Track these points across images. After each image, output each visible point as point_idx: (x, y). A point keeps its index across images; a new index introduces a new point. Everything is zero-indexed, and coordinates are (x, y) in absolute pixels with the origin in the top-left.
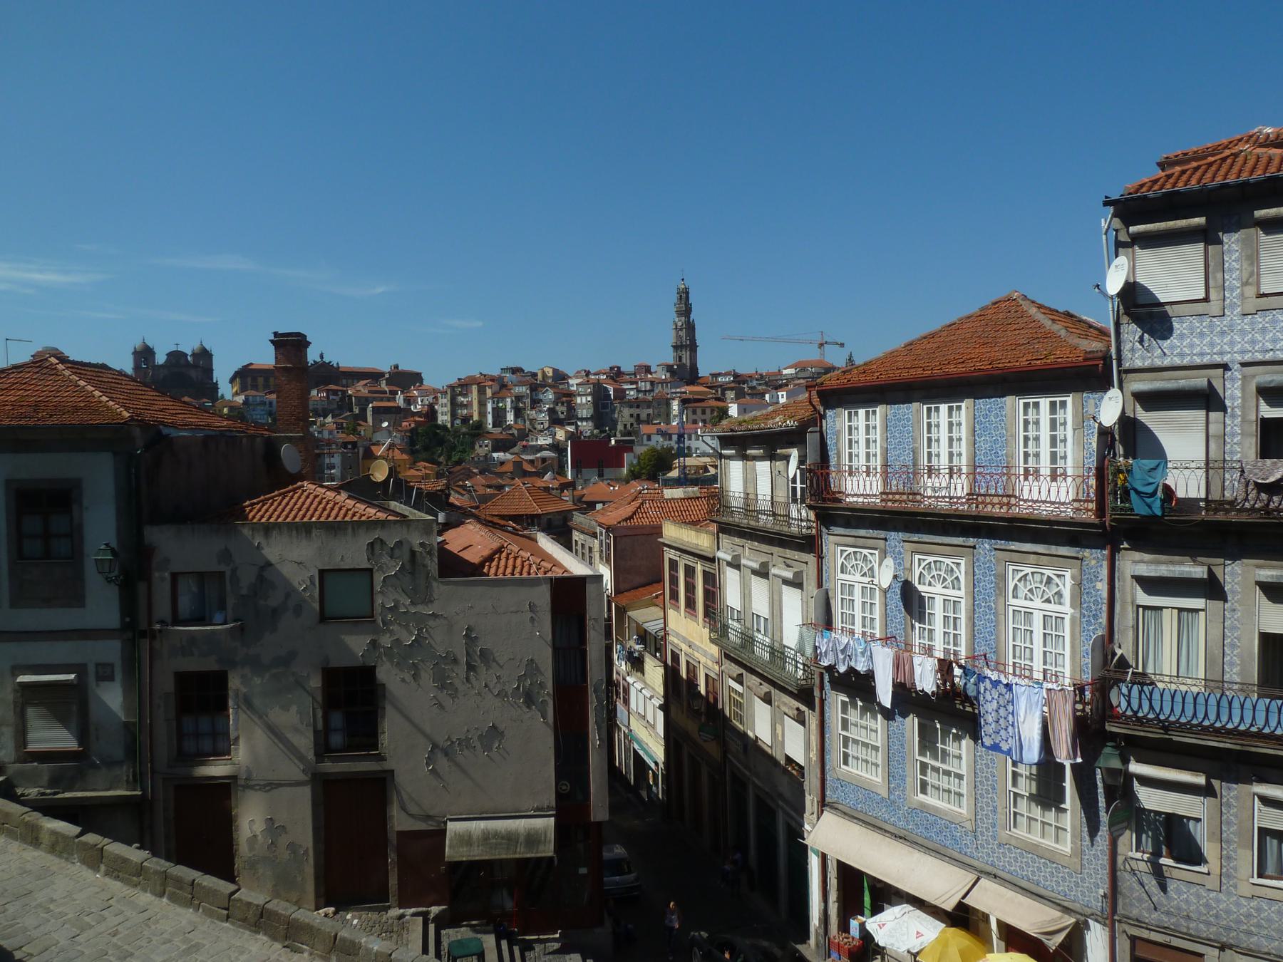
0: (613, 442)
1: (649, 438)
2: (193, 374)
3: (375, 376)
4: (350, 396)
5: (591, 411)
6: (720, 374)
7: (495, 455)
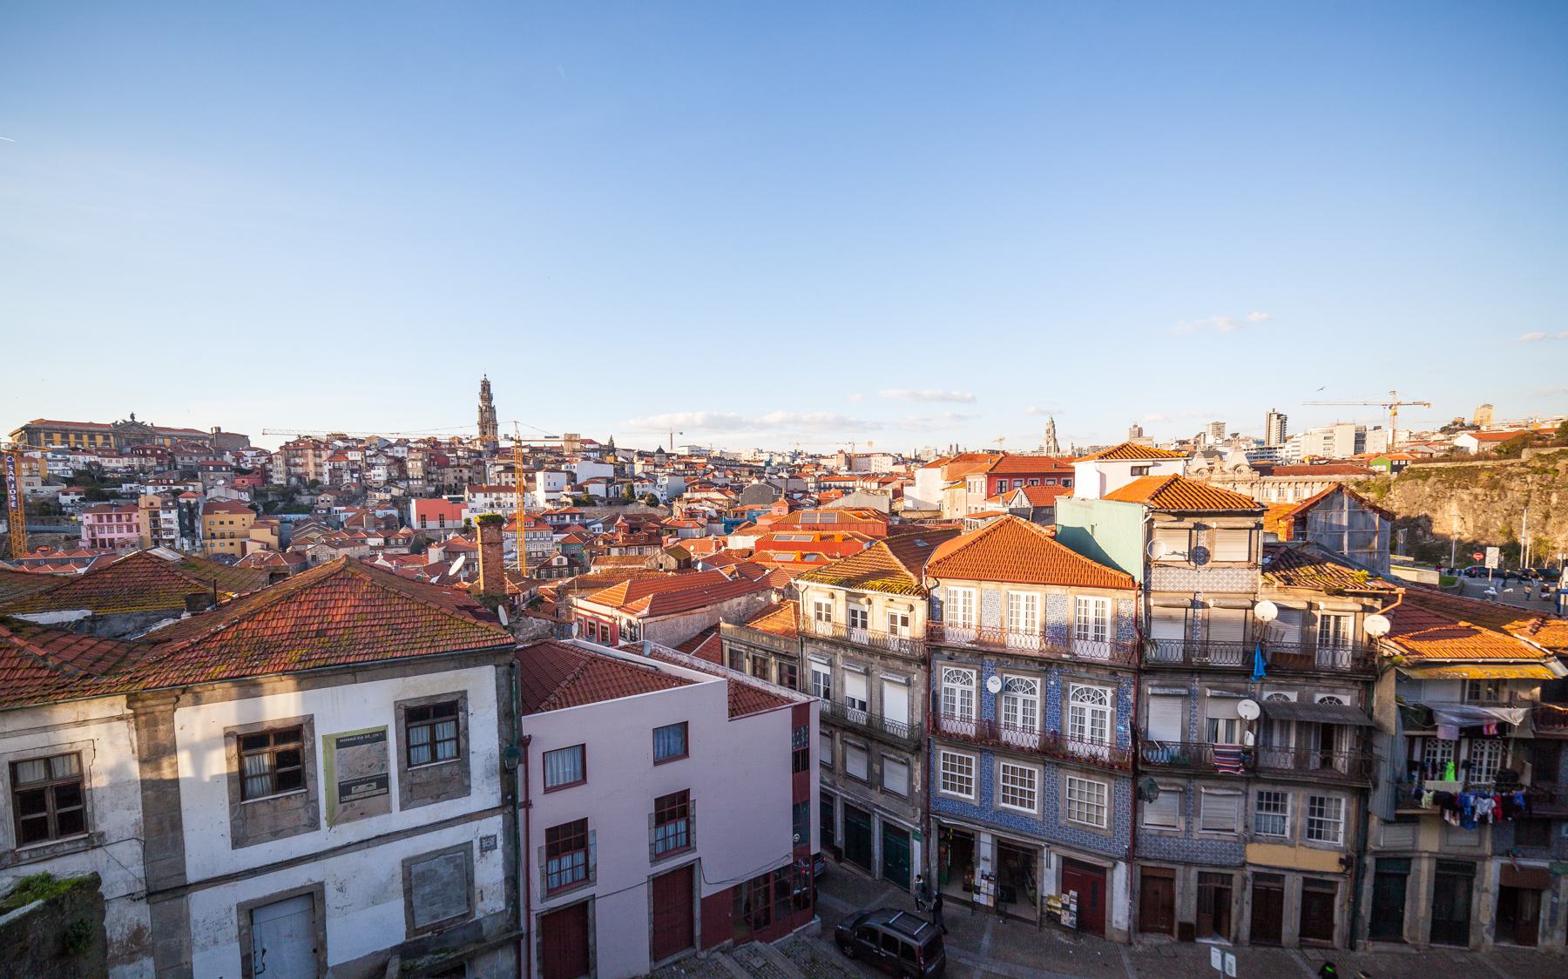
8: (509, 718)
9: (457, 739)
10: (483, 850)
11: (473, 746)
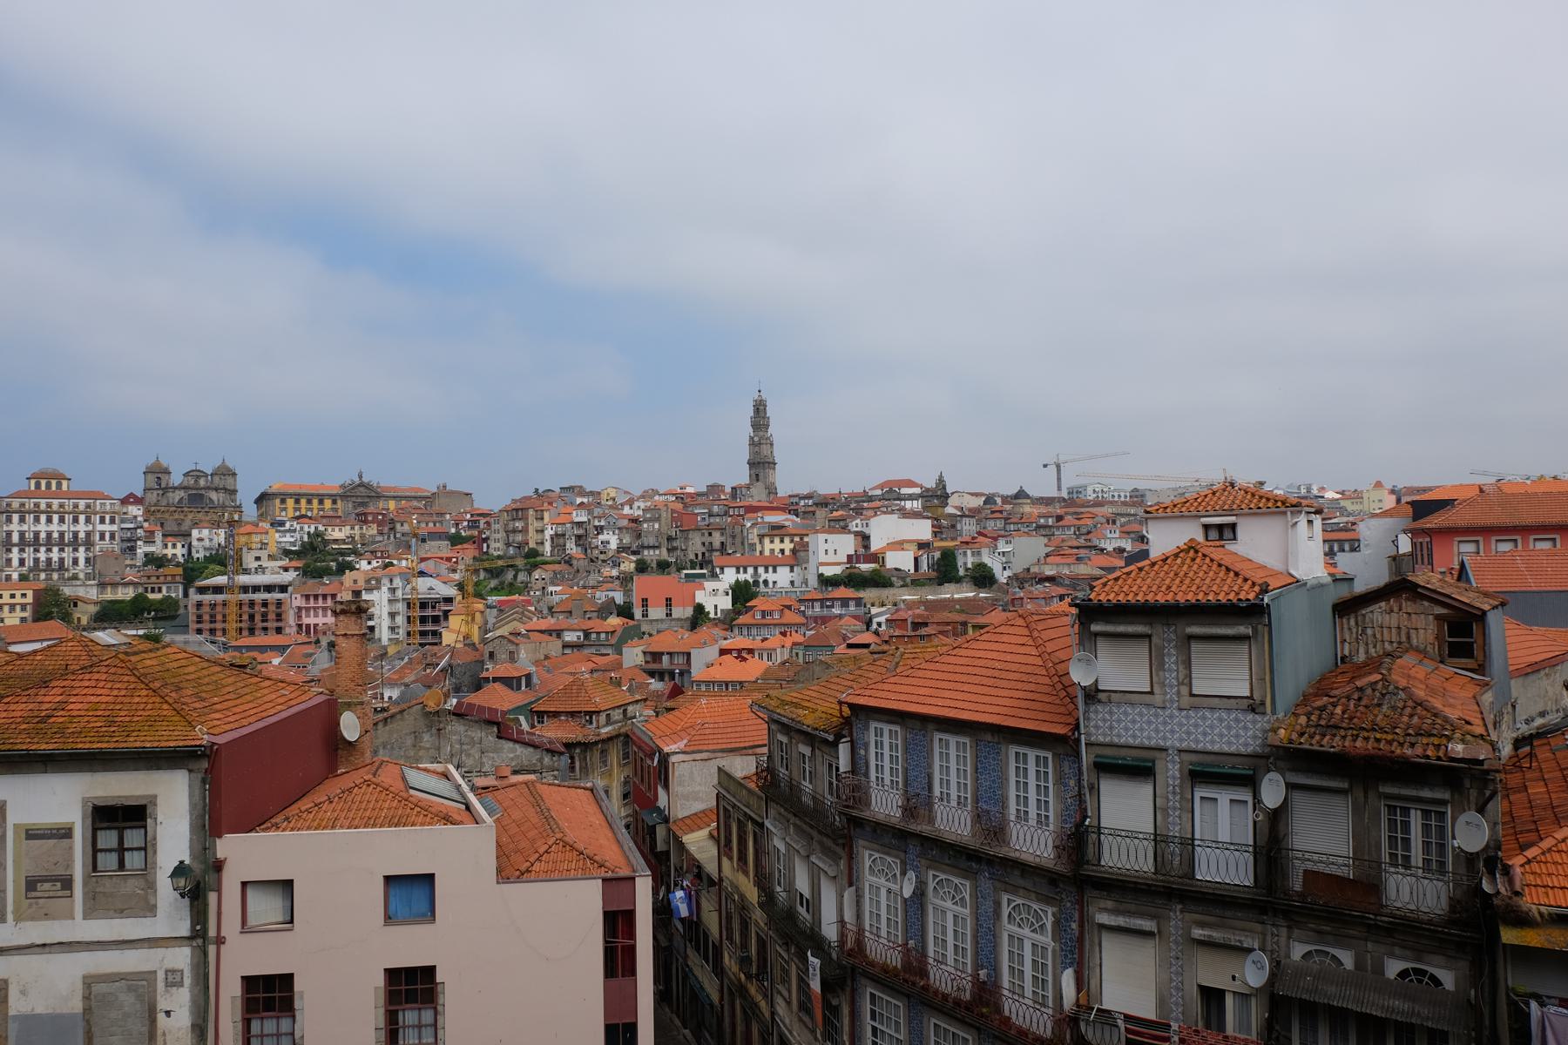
2: (214, 496)
4: (392, 521)
7: (551, 589)
9: (145, 849)
10: (169, 985)
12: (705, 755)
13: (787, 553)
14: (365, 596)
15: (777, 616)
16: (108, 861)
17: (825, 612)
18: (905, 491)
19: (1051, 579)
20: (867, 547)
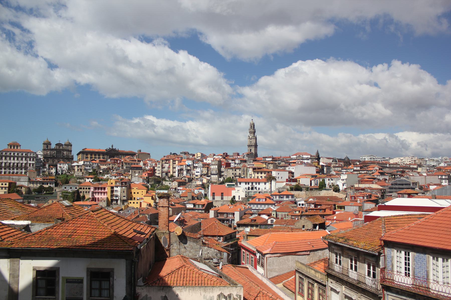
0: (226, 185)
1: (240, 184)
3: (133, 154)
4: (122, 162)
5: (217, 172)
6: (266, 157)
7: (179, 188)
8: (131, 284)
9: (109, 289)
11: (115, 294)
12: (278, 255)
13: (263, 178)
14: (115, 189)
15: (264, 200)
16: (96, 293)
17: (281, 199)
18: (305, 156)
19: (363, 189)
20: (293, 177)
